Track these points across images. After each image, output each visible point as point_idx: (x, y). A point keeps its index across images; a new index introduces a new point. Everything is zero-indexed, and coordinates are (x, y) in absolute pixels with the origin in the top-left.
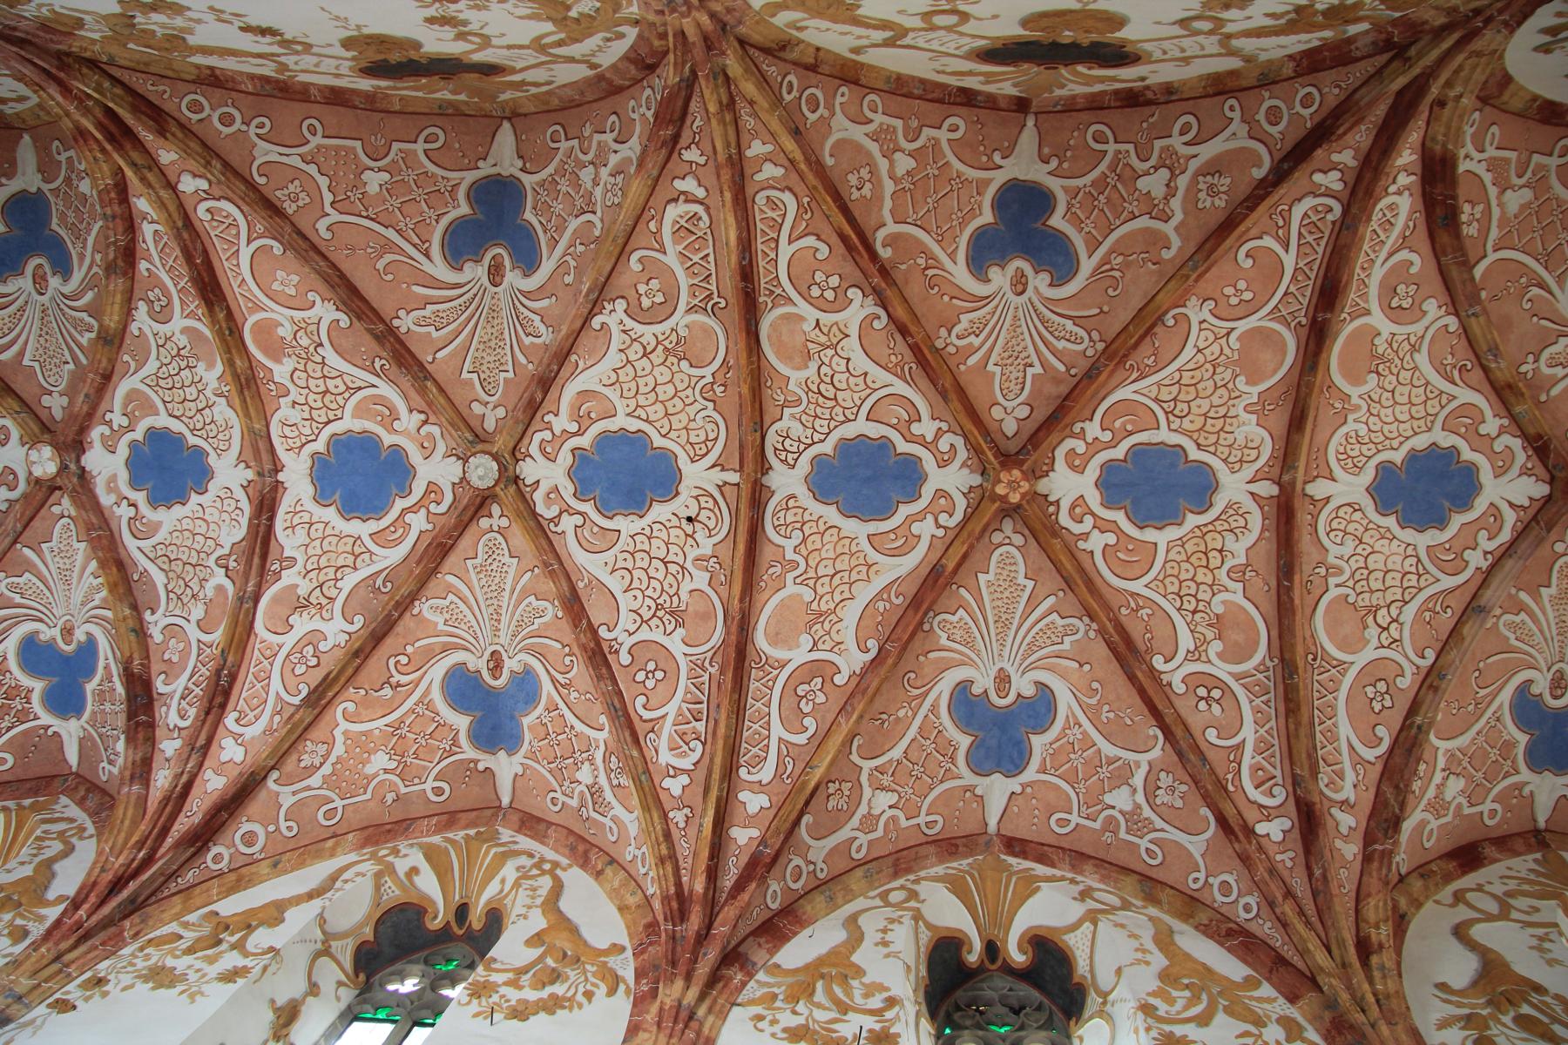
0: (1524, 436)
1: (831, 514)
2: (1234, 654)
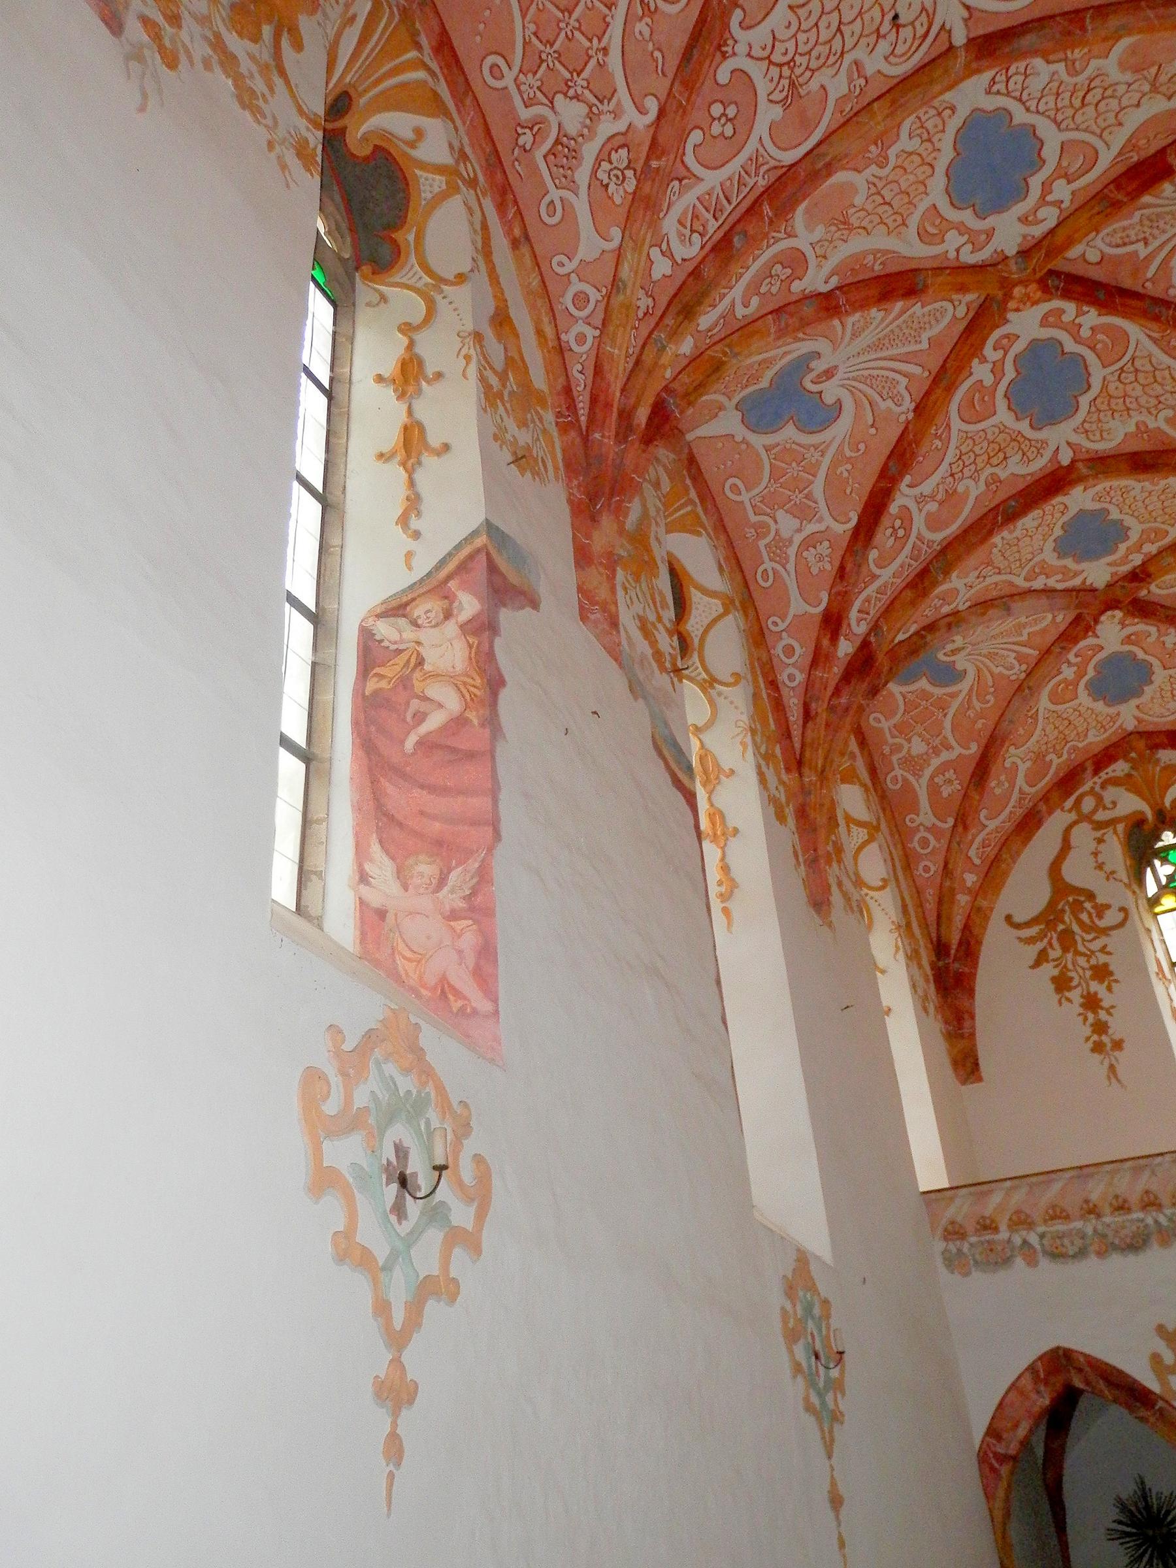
0: (1144, 564)
1: (947, 154)
2: (934, 523)
